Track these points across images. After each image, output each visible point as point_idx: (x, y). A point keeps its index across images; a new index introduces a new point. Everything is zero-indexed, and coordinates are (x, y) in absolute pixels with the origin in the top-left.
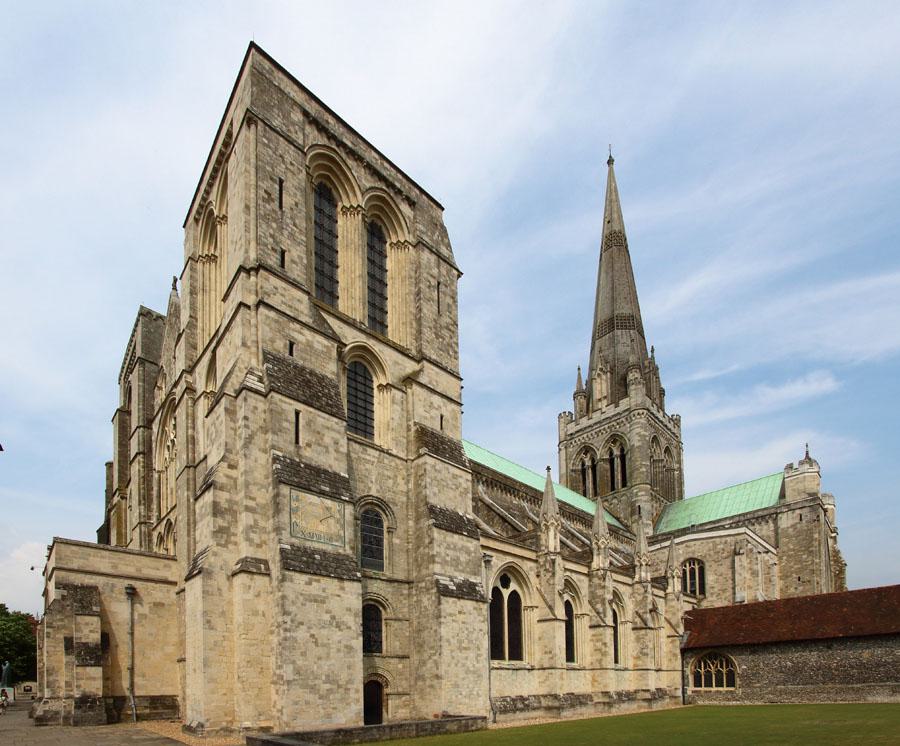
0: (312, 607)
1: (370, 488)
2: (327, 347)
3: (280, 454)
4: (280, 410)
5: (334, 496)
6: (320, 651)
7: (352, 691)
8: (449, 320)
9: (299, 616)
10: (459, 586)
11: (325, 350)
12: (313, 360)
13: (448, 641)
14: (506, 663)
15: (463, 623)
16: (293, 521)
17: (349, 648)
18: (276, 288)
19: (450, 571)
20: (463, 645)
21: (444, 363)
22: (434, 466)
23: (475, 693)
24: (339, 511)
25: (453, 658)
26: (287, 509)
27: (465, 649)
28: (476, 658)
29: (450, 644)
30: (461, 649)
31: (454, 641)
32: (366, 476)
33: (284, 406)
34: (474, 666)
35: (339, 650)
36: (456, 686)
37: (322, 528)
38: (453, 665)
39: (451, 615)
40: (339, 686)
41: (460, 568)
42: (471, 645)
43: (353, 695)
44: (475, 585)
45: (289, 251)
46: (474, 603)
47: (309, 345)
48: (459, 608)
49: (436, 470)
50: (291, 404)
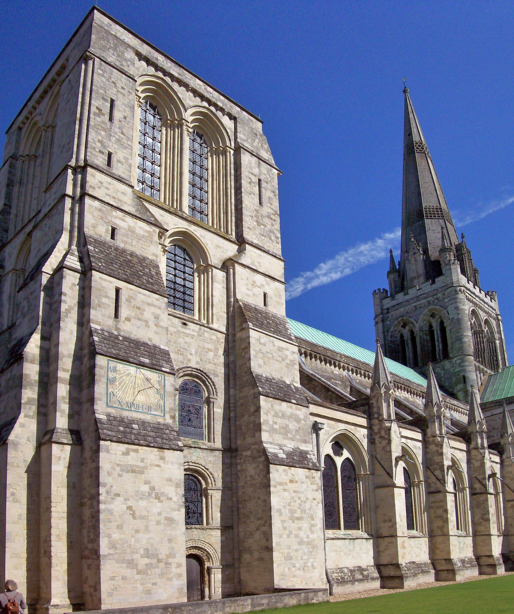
0: (128, 477)
1: (189, 360)
2: (149, 232)
3: (98, 327)
4: (100, 287)
5: (153, 367)
6: (139, 524)
7: (174, 565)
8: (270, 211)
9: (114, 488)
10: (289, 455)
11: (146, 234)
12: (134, 243)
13: (279, 511)
14: (342, 532)
15: (294, 492)
16: (110, 390)
17: (170, 520)
18: (101, 183)
19: (279, 439)
20: (296, 515)
21: (265, 247)
22: (258, 340)
23: (309, 564)
24: (159, 382)
25: (285, 528)
26: (104, 380)
27: (298, 519)
28: (310, 529)
29: (281, 514)
30: (293, 519)
31: (286, 512)
32: (185, 349)
33: (104, 284)
34: (308, 537)
35: (158, 523)
37: (141, 399)
38: (285, 536)
39: (281, 484)
40: (159, 561)
42: (305, 516)
43: (174, 570)
44: (307, 453)
45: (116, 153)
46: (307, 470)
47: (131, 230)
48: (290, 477)
49: (260, 343)
50: (111, 282)
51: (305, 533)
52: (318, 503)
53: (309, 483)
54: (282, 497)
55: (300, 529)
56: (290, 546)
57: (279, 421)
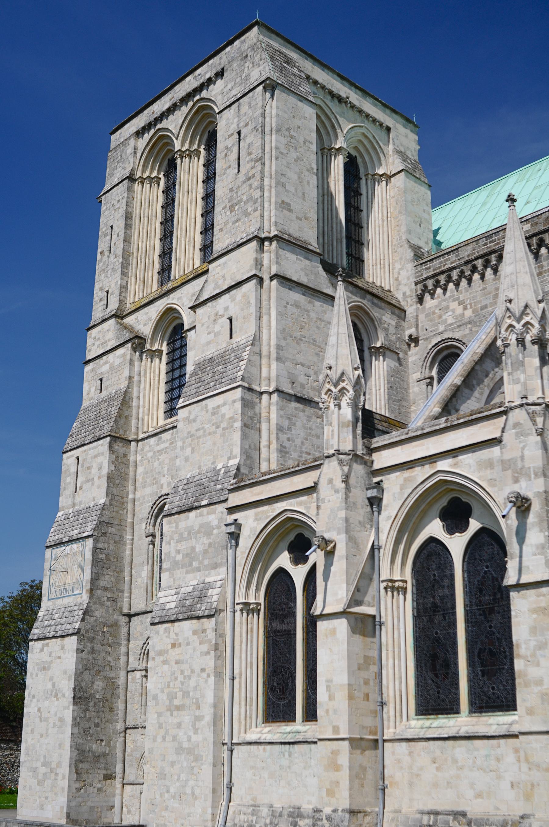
15: (177, 662)
20: (176, 702)
27: (179, 708)
28: (194, 725)
29: (157, 704)
31: (162, 698)
34: (189, 740)
36: (162, 776)
38: (159, 740)
41: (195, 564)
46: (194, 621)
51: (185, 733)
52: (208, 676)
53: (197, 642)
54: (160, 674)
56: (165, 756)
57: (183, 546)
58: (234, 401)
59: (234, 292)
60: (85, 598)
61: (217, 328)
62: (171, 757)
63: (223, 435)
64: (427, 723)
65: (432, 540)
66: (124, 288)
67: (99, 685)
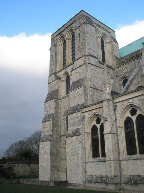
15: (73, 146)
27: (74, 155)
28: (77, 159)
31: (70, 153)
34: (76, 162)
36: (71, 170)
38: (70, 162)
39: (69, 144)
46: (76, 136)
52: (80, 148)
55: (74, 159)
57: (72, 121)
58: (82, 90)
59: (80, 67)
60: (51, 133)
61: (77, 75)
62: (73, 166)
63: (80, 97)
64: (130, 156)
65: (128, 117)
66: (56, 68)
67: (55, 151)
